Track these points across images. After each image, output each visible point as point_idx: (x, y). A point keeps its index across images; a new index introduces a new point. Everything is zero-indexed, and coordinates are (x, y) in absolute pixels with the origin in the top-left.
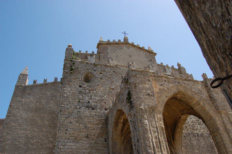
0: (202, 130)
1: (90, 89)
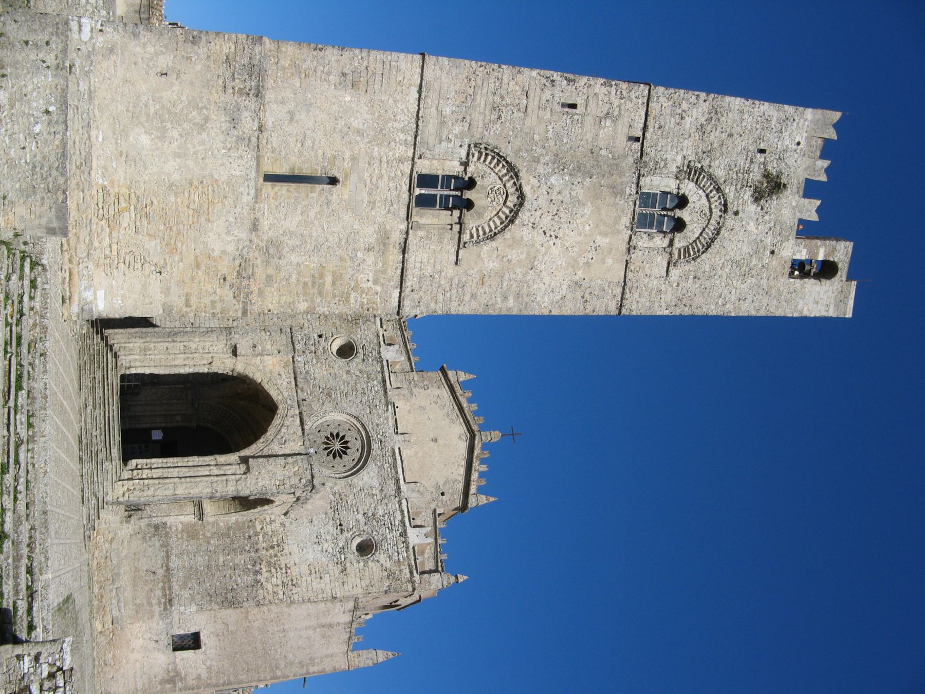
0: (270, 587)
1: (320, 352)
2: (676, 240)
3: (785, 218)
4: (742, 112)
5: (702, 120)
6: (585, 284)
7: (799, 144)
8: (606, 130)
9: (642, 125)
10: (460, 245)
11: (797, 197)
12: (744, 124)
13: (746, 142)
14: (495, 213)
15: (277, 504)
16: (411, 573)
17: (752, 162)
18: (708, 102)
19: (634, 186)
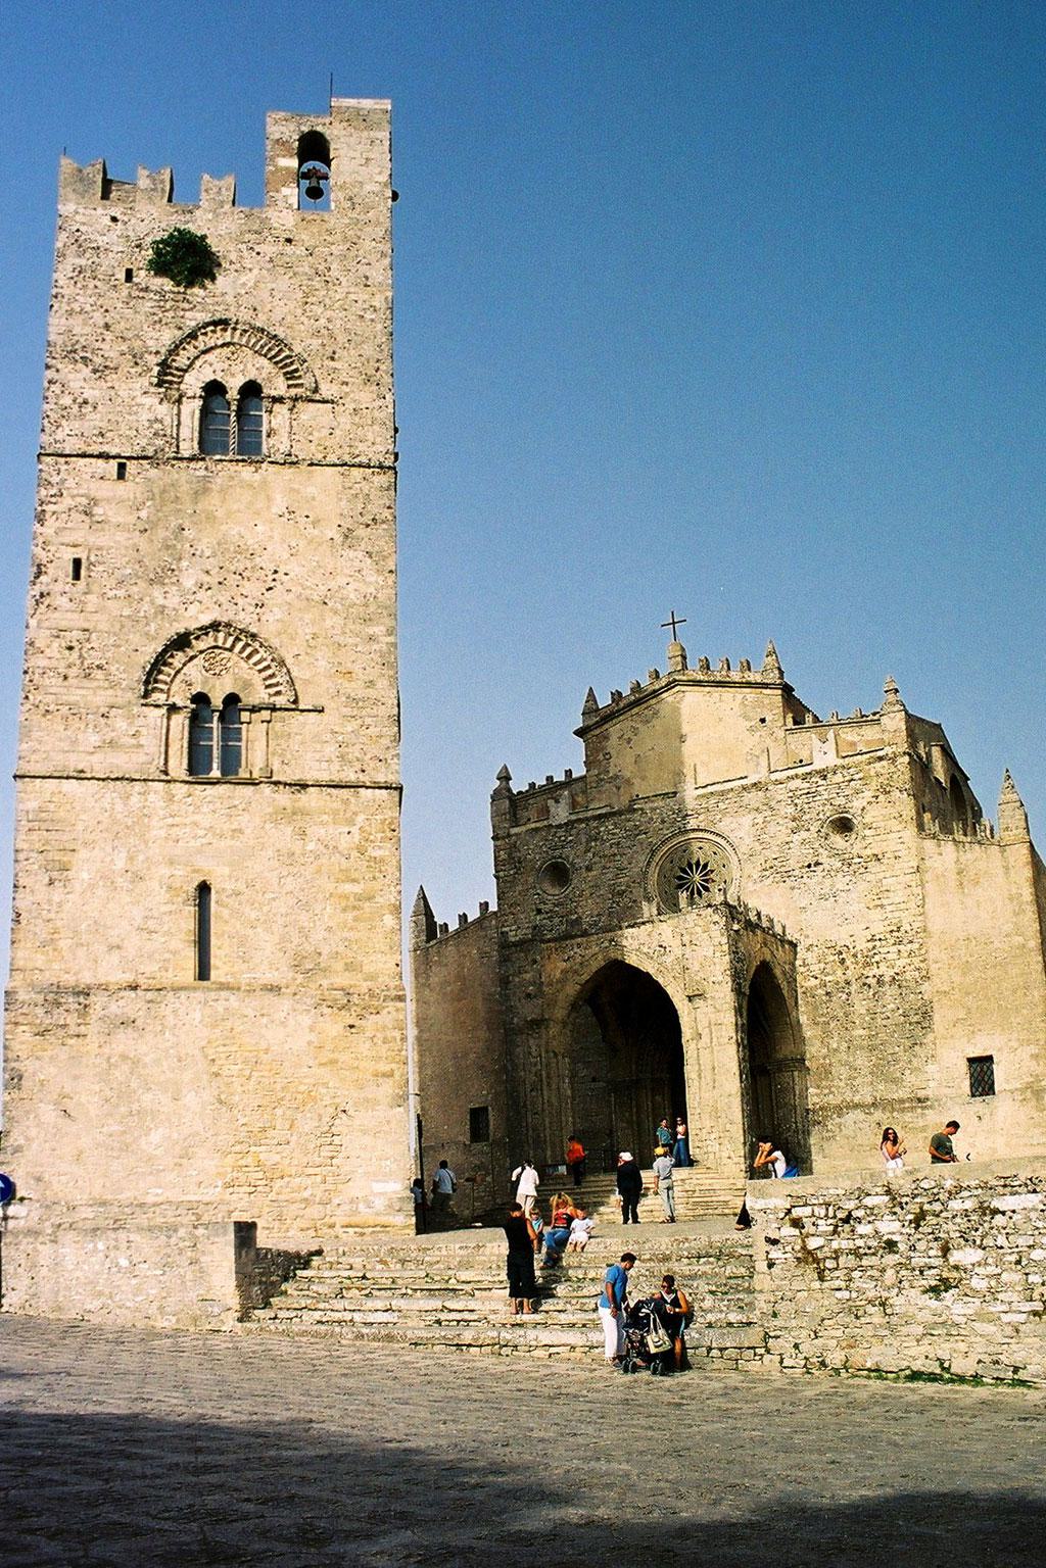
2: (274, 393)
3: (234, 228)
4: (71, 313)
5: (86, 371)
6: (347, 523)
7: (114, 219)
8: (110, 513)
9: (100, 461)
10: (294, 706)
11: (198, 213)
12: (88, 308)
13: (115, 300)
14: (243, 664)
15: (768, 958)
17: (146, 289)
18: (59, 366)
19: (193, 465)
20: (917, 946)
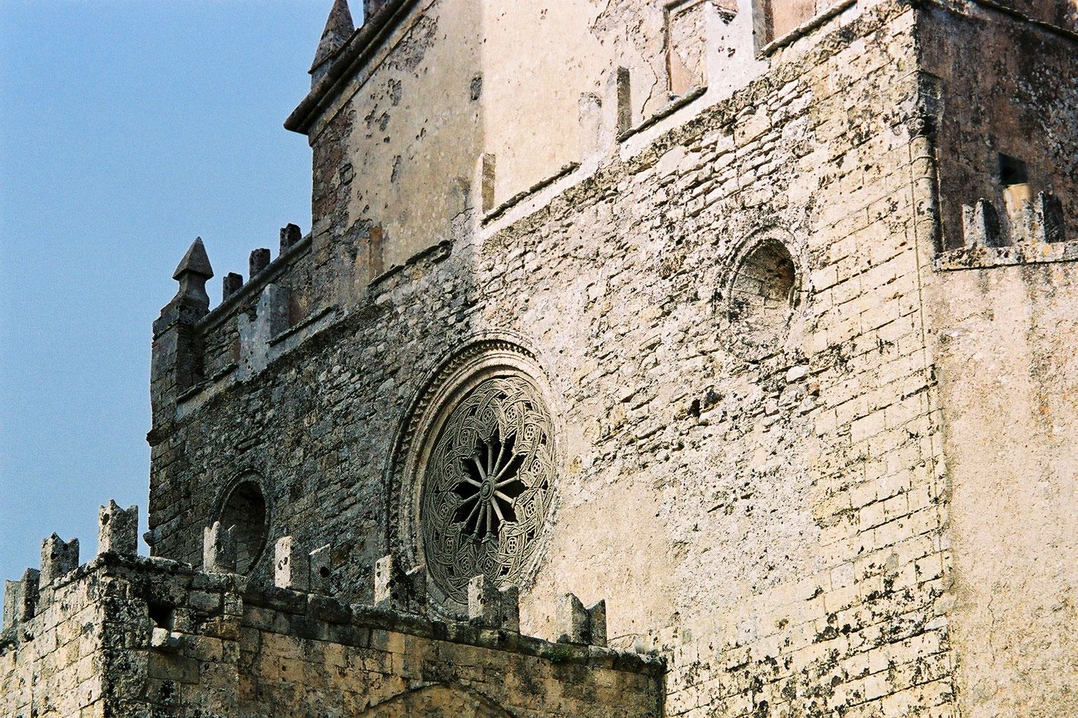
16: (848, 35)
20: (931, 642)
